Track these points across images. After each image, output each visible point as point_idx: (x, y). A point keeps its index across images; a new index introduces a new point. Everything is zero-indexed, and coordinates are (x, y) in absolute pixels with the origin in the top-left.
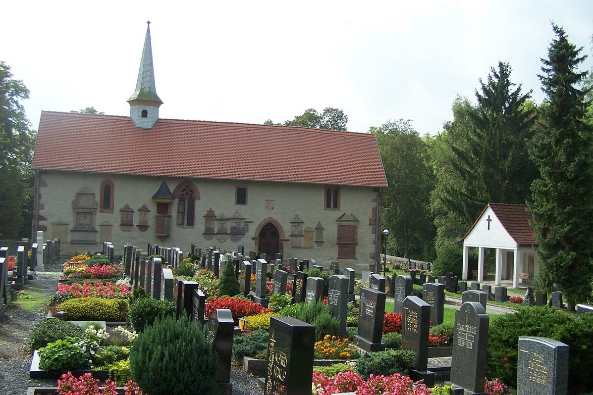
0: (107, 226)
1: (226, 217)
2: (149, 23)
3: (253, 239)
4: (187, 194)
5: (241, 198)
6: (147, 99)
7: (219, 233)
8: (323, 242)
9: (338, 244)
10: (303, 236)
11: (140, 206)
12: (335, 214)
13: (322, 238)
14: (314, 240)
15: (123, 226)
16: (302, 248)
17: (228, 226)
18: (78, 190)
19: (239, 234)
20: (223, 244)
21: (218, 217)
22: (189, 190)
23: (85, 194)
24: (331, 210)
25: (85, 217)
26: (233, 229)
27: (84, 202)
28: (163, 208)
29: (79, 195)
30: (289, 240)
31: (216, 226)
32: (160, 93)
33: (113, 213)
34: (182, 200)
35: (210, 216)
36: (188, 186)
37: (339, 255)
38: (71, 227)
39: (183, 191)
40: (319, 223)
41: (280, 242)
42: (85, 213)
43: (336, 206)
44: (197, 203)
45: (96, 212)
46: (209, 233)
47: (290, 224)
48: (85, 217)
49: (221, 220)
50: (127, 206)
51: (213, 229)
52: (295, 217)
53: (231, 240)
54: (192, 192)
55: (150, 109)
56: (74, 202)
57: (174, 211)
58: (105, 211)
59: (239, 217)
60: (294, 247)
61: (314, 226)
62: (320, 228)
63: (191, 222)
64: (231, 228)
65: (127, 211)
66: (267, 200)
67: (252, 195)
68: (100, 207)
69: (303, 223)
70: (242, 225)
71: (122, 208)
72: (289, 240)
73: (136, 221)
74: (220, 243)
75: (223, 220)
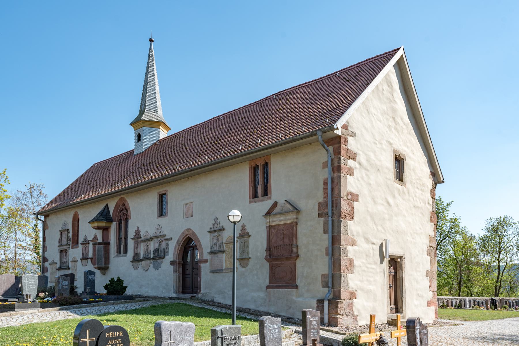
0: (74, 261)
1: (149, 237)
2: (151, 40)
3: (172, 263)
12: (265, 205)
13: (248, 253)
15: (83, 261)
17: (153, 246)
21: (142, 238)
24: (259, 201)
30: (206, 261)
38: (58, 266)
43: (266, 193)
46: (136, 259)
47: (209, 234)
50: (86, 238)
52: (213, 222)
53: (154, 267)
60: (213, 271)
64: (153, 251)
66: (186, 205)
69: (224, 229)
72: (206, 261)
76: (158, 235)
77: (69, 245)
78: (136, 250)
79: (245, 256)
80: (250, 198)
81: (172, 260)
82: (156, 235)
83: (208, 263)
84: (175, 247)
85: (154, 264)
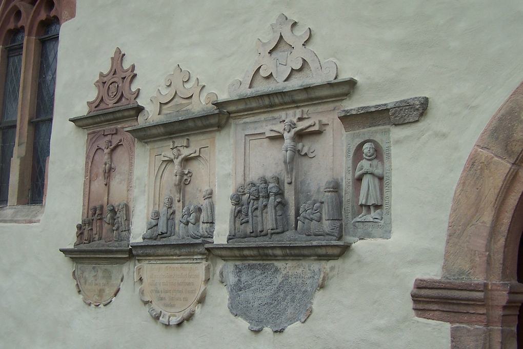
1: (200, 105)
3: (430, 299)
17: (227, 167)
19: (296, 253)
20: (173, 338)
21: (152, 115)
31: (144, 188)
46: (100, 246)
53: (238, 309)
59: (296, 83)
64: (237, 200)
74: (156, 330)
76: (278, 84)
78: (98, 185)
81: (433, 272)
82: (263, 87)
84: (475, 168)
85: (238, 288)
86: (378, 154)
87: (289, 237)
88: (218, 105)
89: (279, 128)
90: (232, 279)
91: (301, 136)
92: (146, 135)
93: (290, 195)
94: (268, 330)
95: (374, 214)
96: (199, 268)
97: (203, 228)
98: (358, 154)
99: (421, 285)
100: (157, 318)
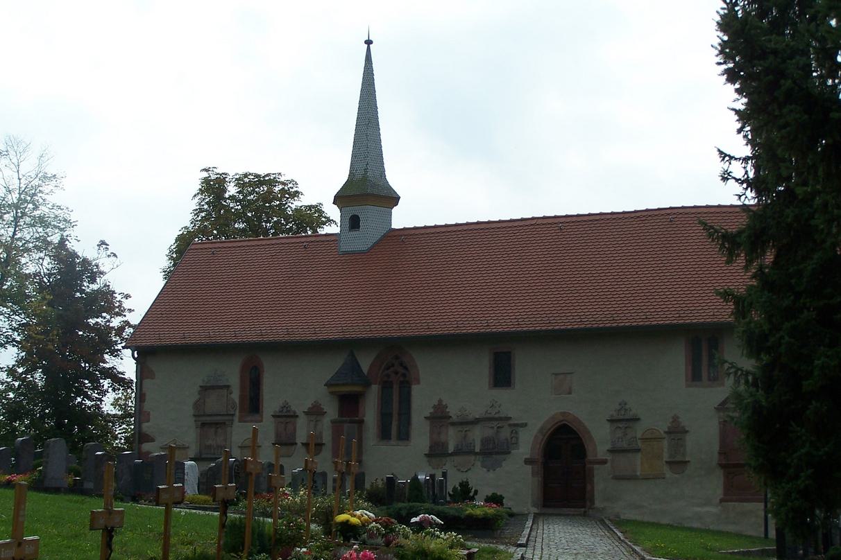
1: (471, 417)
2: (369, 42)
3: (527, 462)
4: (397, 373)
5: (502, 376)
6: (367, 190)
7: (457, 452)
8: (686, 462)
9: (722, 466)
10: (638, 450)
11: (308, 404)
14: (665, 459)
16: (632, 478)
17: (477, 436)
18: (203, 381)
19: (497, 453)
21: (454, 418)
22: (401, 364)
23: (213, 388)
25: (216, 432)
26: (485, 441)
27: (214, 404)
28: (349, 404)
29: (205, 389)
30: (604, 462)
31: (452, 439)
32: (395, 177)
33: (261, 421)
34: (386, 386)
35: (439, 417)
36: (397, 358)
37: (725, 494)
39: (388, 368)
40: (675, 419)
41: (588, 466)
42: (210, 424)
44: (415, 389)
45: (233, 420)
46: (436, 452)
47: (608, 425)
48: (216, 432)
49: (461, 424)
50: (286, 406)
51: (444, 445)
52: (618, 407)
53: (483, 466)
54: (406, 368)
55: (368, 214)
56: (196, 405)
57: (370, 412)
58: (249, 419)
59: (497, 416)
60: (618, 478)
61: (663, 427)
62: (677, 432)
63: (404, 436)
64: (482, 441)
65: (286, 416)
66: (556, 374)
67: (525, 365)
68: (240, 412)
69: (639, 419)
70: (505, 433)
71: (277, 410)
72: (604, 462)
73: (301, 436)
75: (466, 423)
77: (233, 415)
79: (679, 458)
80: (687, 380)
81: (528, 456)
82: (488, 416)
83: (609, 465)
86: (516, 433)
87: (496, 450)
88: (477, 419)
89: (493, 425)
90: (481, 459)
91: (498, 427)
92: (453, 424)
93: (496, 441)
94: (491, 471)
95: (515, 445)
96: (473, 458)
97: (473, 448)
98: (512, 432)
99: (526, 459)
100: (459, 470)
